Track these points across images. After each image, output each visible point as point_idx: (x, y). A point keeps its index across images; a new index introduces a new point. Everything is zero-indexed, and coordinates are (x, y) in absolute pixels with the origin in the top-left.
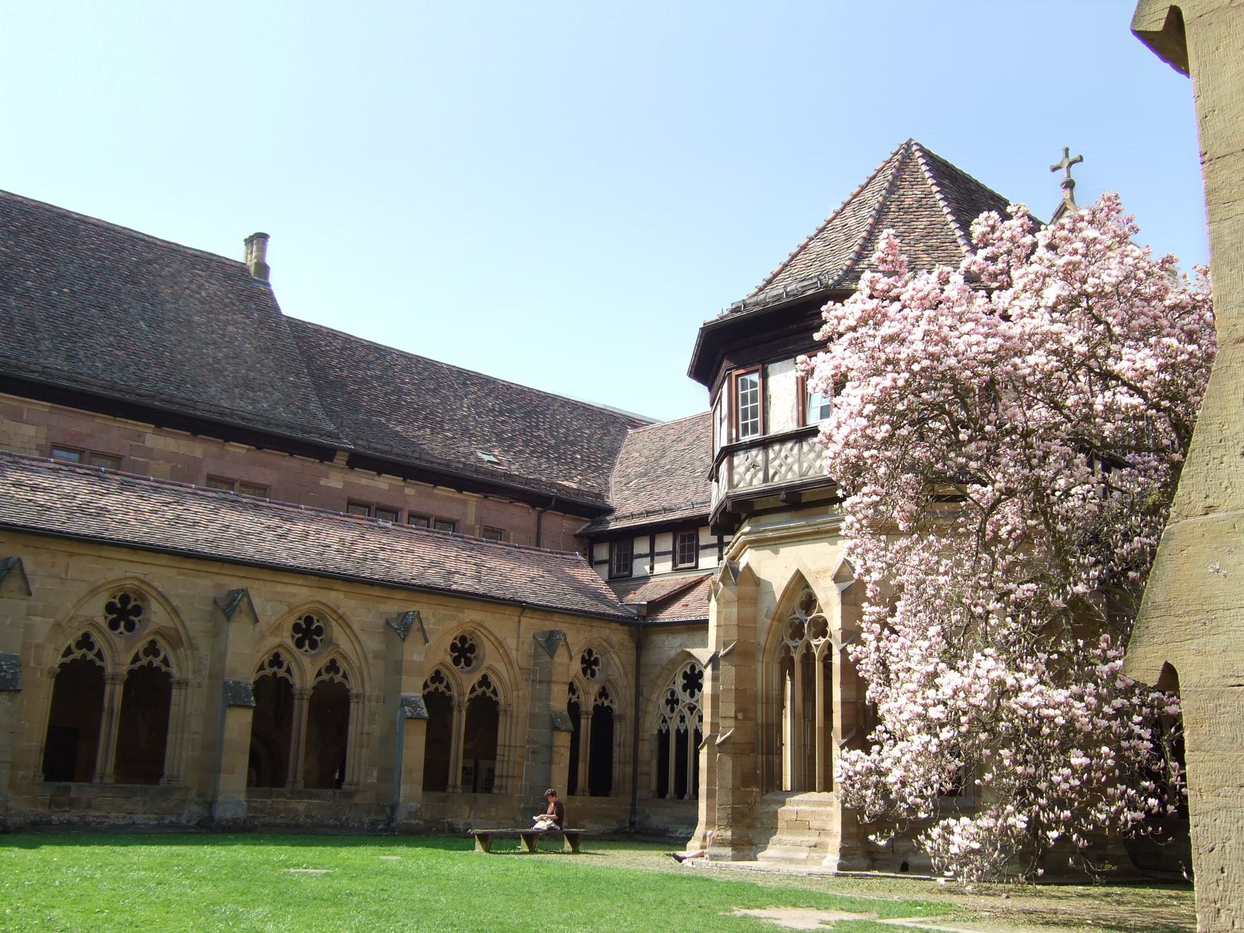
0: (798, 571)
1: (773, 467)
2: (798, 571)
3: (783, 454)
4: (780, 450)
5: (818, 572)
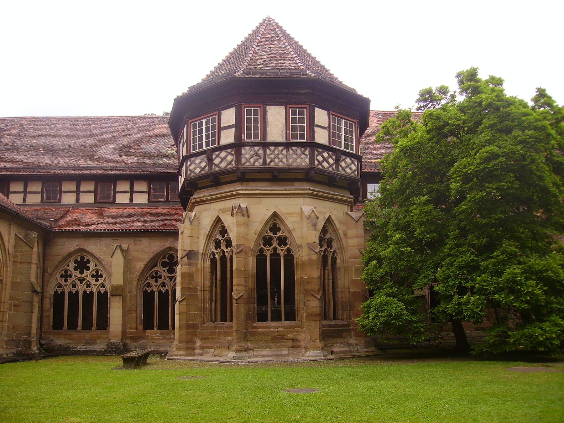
0: (275, 211)
2: (275, 211)
3: (276, 152)
5: (288, 214)
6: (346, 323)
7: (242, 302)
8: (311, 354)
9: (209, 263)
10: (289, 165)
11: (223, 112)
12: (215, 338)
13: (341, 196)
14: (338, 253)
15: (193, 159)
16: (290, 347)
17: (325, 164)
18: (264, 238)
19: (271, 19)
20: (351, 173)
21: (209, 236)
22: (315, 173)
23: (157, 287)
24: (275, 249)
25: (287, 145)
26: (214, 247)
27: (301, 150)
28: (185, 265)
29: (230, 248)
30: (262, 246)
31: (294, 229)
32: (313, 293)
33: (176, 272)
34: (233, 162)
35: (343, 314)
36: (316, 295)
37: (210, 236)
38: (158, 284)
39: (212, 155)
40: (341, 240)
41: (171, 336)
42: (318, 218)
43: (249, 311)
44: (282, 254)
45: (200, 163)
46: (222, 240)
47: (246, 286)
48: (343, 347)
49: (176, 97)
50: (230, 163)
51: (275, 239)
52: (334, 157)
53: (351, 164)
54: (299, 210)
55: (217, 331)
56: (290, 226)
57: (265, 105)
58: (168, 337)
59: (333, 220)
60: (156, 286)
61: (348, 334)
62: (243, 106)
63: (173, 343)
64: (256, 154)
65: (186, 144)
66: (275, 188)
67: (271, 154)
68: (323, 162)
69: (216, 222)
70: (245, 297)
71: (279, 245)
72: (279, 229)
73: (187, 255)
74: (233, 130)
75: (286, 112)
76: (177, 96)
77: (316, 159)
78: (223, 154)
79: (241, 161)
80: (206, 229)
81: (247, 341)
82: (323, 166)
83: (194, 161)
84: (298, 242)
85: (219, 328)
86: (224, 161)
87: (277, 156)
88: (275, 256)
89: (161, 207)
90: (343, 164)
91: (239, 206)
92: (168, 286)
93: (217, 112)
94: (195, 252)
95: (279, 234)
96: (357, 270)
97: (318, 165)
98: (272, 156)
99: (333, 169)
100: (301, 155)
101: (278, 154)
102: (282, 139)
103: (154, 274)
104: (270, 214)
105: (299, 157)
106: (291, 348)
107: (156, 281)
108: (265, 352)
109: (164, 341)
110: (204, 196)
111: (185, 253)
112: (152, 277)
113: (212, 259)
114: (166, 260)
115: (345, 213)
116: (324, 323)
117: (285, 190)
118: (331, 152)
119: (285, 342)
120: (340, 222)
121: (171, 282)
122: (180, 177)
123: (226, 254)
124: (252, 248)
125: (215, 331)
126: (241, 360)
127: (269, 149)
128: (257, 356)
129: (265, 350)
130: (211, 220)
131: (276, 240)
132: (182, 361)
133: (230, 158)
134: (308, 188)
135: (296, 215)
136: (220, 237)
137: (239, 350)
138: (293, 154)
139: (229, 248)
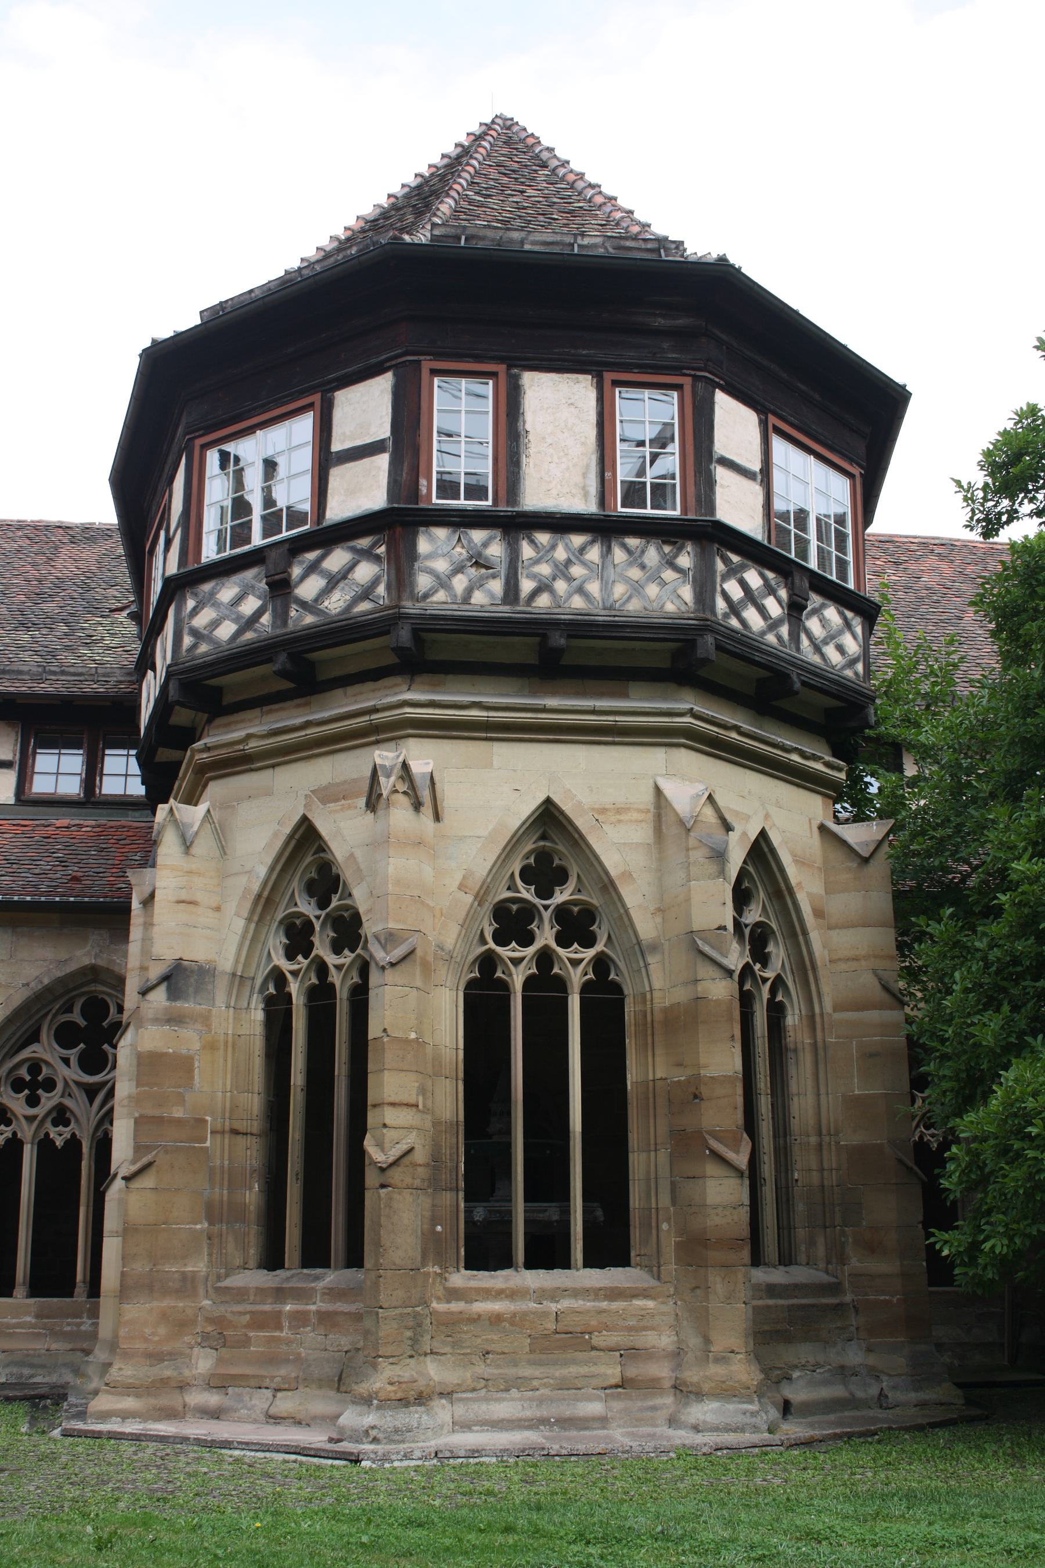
0: (548, 801)
1: (533, 576)
2: (548, 801)
3: (561, 554)
5: (603, 811)
6: (822, 1277)
7: (408, 1180)
8: (710, 1418)
9: (259, 1015)
10: (611, 608)
12: (279, 1338)
13: (803, 754)
14: (790, 983)
15: (207, 587)
16: (613, 1381)
17: (751, 615)
18: (500, 912)
19: (509, 123)
20: (843, 668)
21: (263, 901)
22: (719, 648)
23: (36, 1123)
24: (545, 958)
26: (281, 952)
27: (659, 549)
28: (156, 1021)
29: (353, 951)
30: (492, 945)
31: (627, 875)
33: (114, 1067)
34: (381, 590)
35: (812, 1243)
36: (730, 1155)
37: (268, 900)
38: (40, 1111)
39: (290, 564)
40: (805, 933)
41: (83, 1323)
42: (728, 828)
43: (434, 1221)
44: (576, 978)
45: (239, 600)
46: (318, 917)
47: (426, 1111)
48: (826, 1383)
49: (148, 344)
50: (366, 594)
51: (547, 915)
52: (783, 593)
53: (840, 632)
54: (647, 797)
55: (288, 1308)
56: (612, 861)
57: (516, 366)
58: (69, 1328)
59: (773, 850)
60: (30, 1119)
61: (839, 1324)
62: (427, 365)
63: (91, 1358)
64: (479, 562)
65: (179, 532)
66: (552, 702)
67: (537, 562)
68: (745, 607)
69: (293, 843)
70: (420, 1156)
71: (563, 940)
72: (561, 877)
73: (166, 978)
74: (383, 461)
75: (600, 399)
76: (153, 341)
77: (719, 589)
78: (337, 559)
79: (412, 584)
80: (249, 872)
81: (426, 1354)
82: (743, 622)
83: (212, 594)
84: (646, 927)
85: (299, 1295)
86: (341, 585)
87: (562, 570)
89: (65, 822)
90: (813, 625)
91: (405, 766)
92: (77, 1120)
93: (316, 398)
94: (201, 968)
95: (561, 896)
96: (871, 1055)
97: (726, 616)
98: (545, 569)
99: (779, 638)
100: (659, 570)
101: (568, 563)
102: (586, 505)
103: (24, 1073)
104: (527, 807)
105: (655, 577)
106: (617, 1386)
107: (33, 1101)
108: (504, 1408)
109: (54, 1346)
110: (249, 736)
111: (156, 972)
112: (18, 1086)
113: (270, 1002)
114: (76, 1017)
115: (815, 825)
116: (761, 1275)
117: (594, 712)
118: (772, 569)
119: (586, 1363)
120: (798, 861)
121: (91, 1105)
122: (150, 673)
123: (335, 978)
124: (451, 948)
126: (402, 1446)
127: (532, 542)
128: (465, 1426)
129: (504, 1395)
130: (276, 835)
131: (551, 920)
132: (127, 1448)
133: (365, 572)
134: (688, 706)
135: (635, 816)
136: (307, 908)
137: (392, 1396)
138: (630, 564)
139: (346, 952)
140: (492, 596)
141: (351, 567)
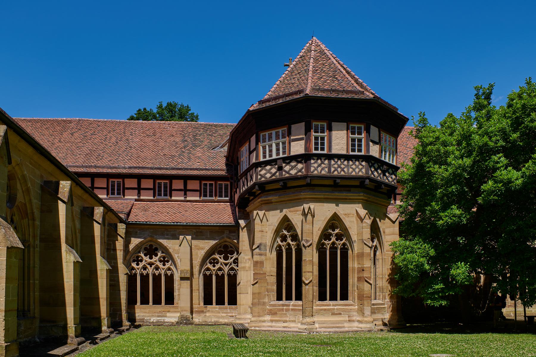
4: (337, 161)
11: (292, 126)
25: (347, 158)
32: (366, 279)
34: (303, 170)
36: (368, 280)
38: (216, 268)
50: (300, 171)
67: (334, 164)
88: (333, 248)
102: (344, 152)
125: (283, 308)
133: (300, 166)
140: (326, 172)
141: (296, 165)
